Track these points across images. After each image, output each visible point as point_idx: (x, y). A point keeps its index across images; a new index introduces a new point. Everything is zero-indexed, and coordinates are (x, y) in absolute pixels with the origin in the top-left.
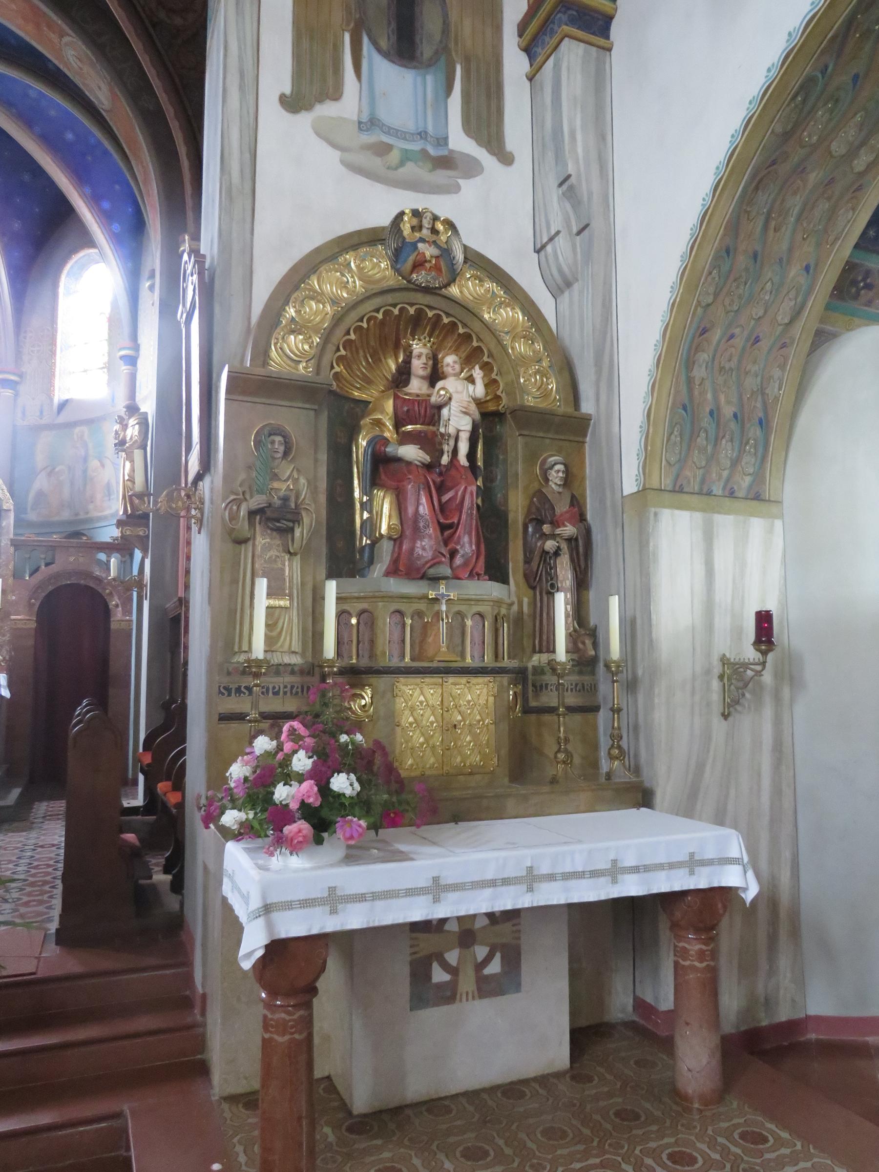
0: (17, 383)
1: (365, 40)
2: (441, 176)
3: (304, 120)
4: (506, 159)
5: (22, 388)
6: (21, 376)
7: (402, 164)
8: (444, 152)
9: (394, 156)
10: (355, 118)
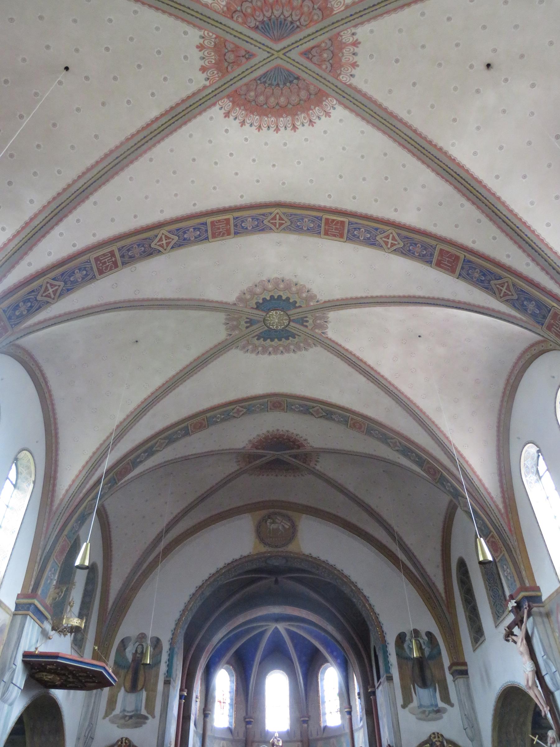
0: (308, 720)
1: (416, 685)
2: (438, 715)
3: (407, 709)
4: (452, 705)
5: (310, 722)
6: (309, 718)
7: (429, 714)
8: (437, 708)
9: (427, 713)
10: (417, 706)
